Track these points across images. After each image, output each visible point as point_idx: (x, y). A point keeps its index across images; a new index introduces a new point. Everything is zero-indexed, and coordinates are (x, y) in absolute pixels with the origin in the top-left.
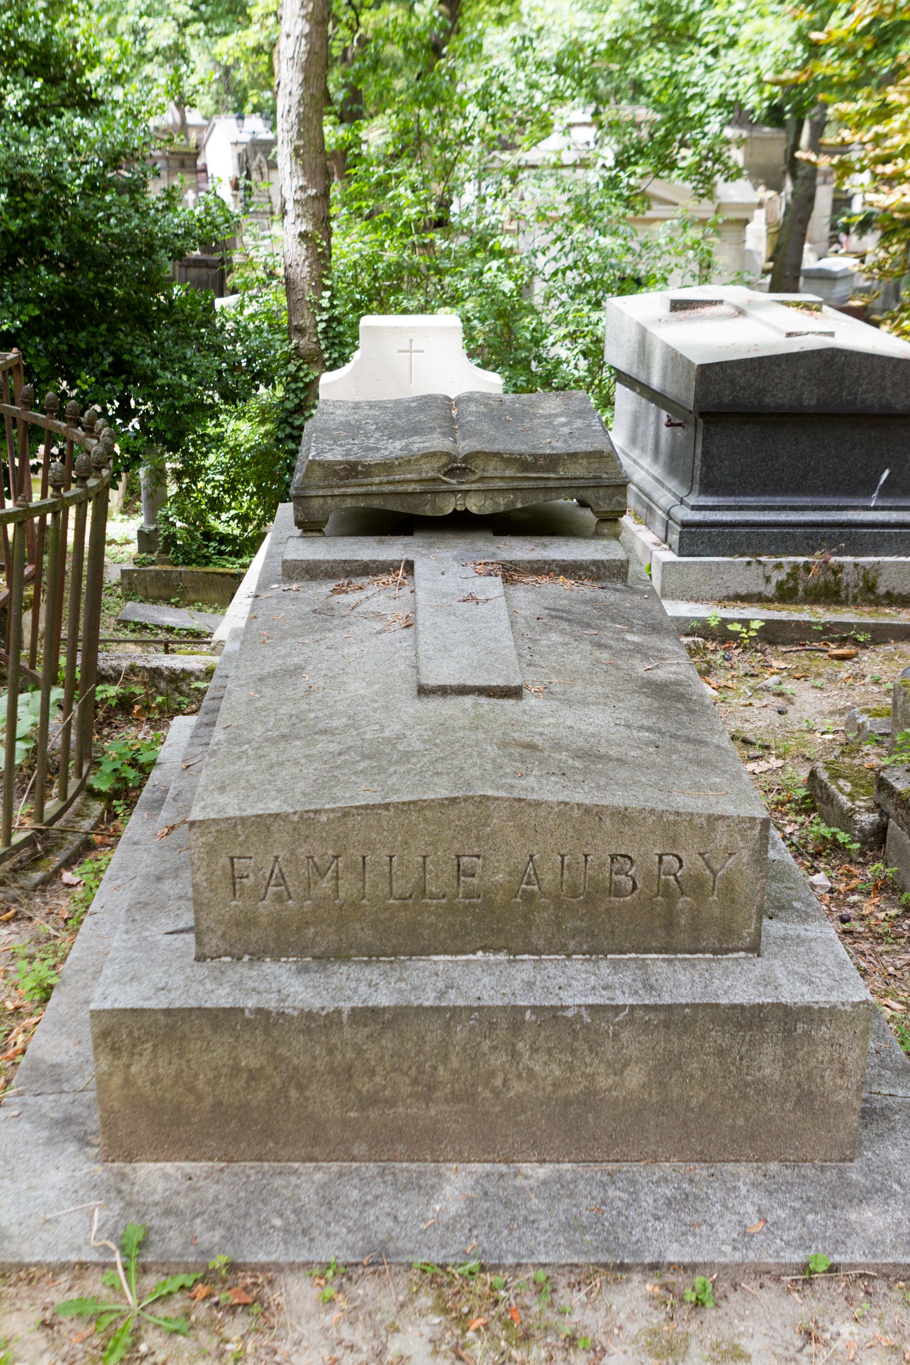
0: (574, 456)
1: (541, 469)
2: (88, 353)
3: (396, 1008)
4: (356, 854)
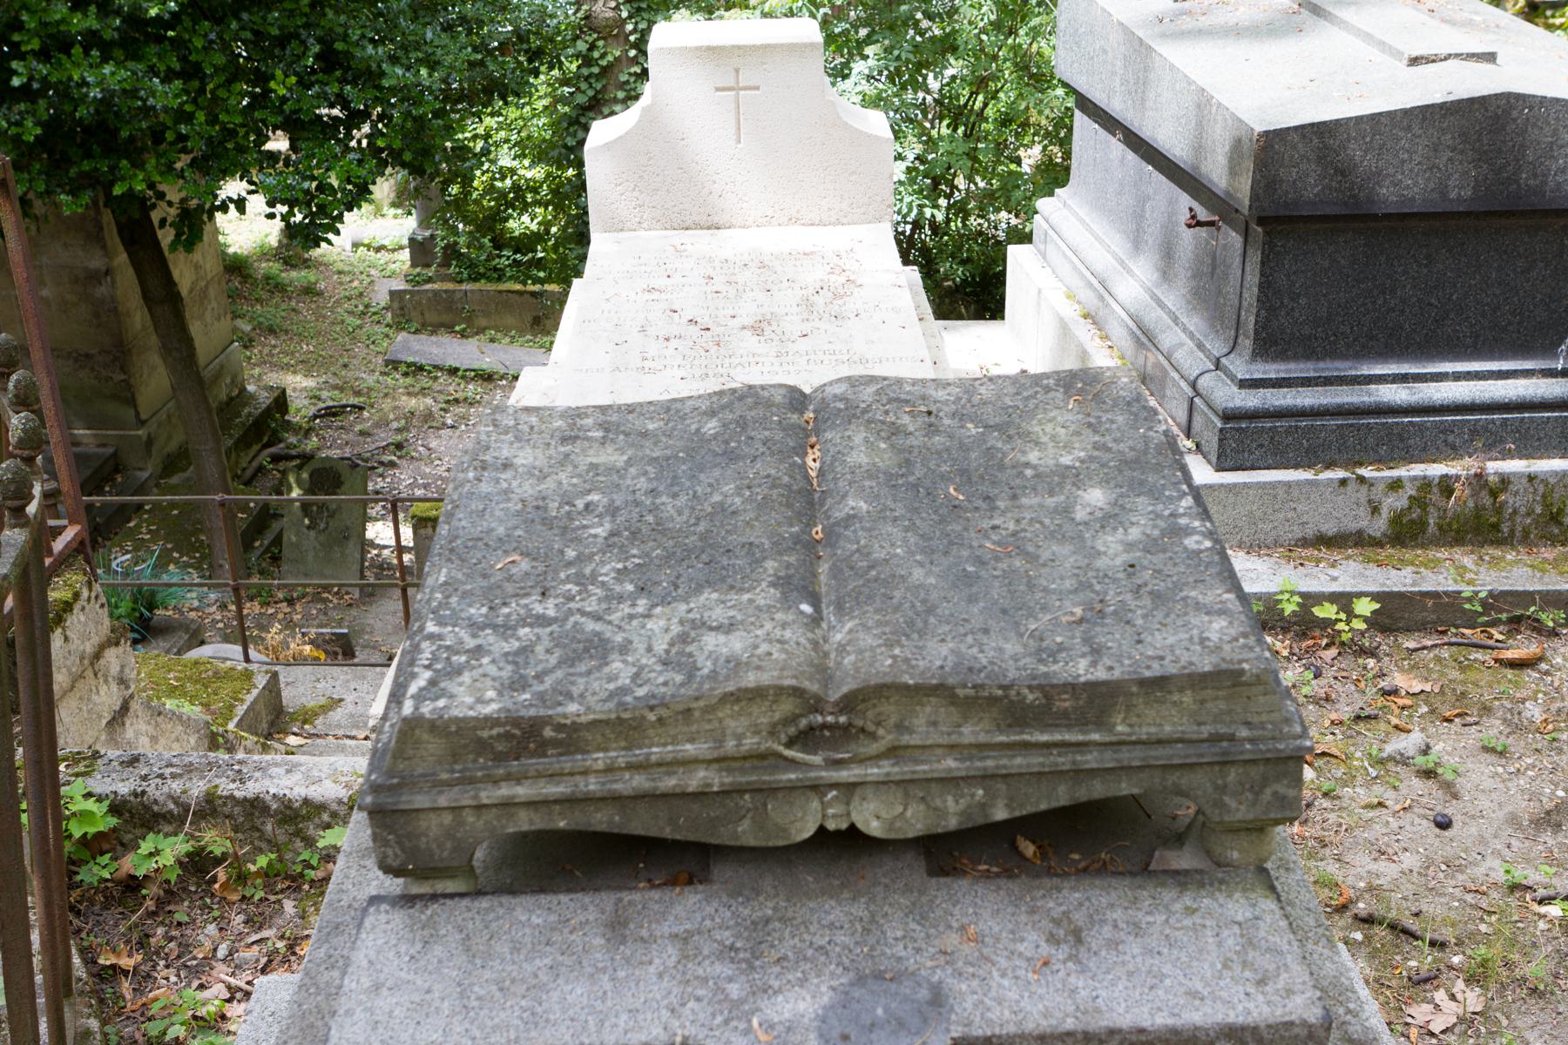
0: (1160, 684)
1: (1066, 720)
2: (282, 41)
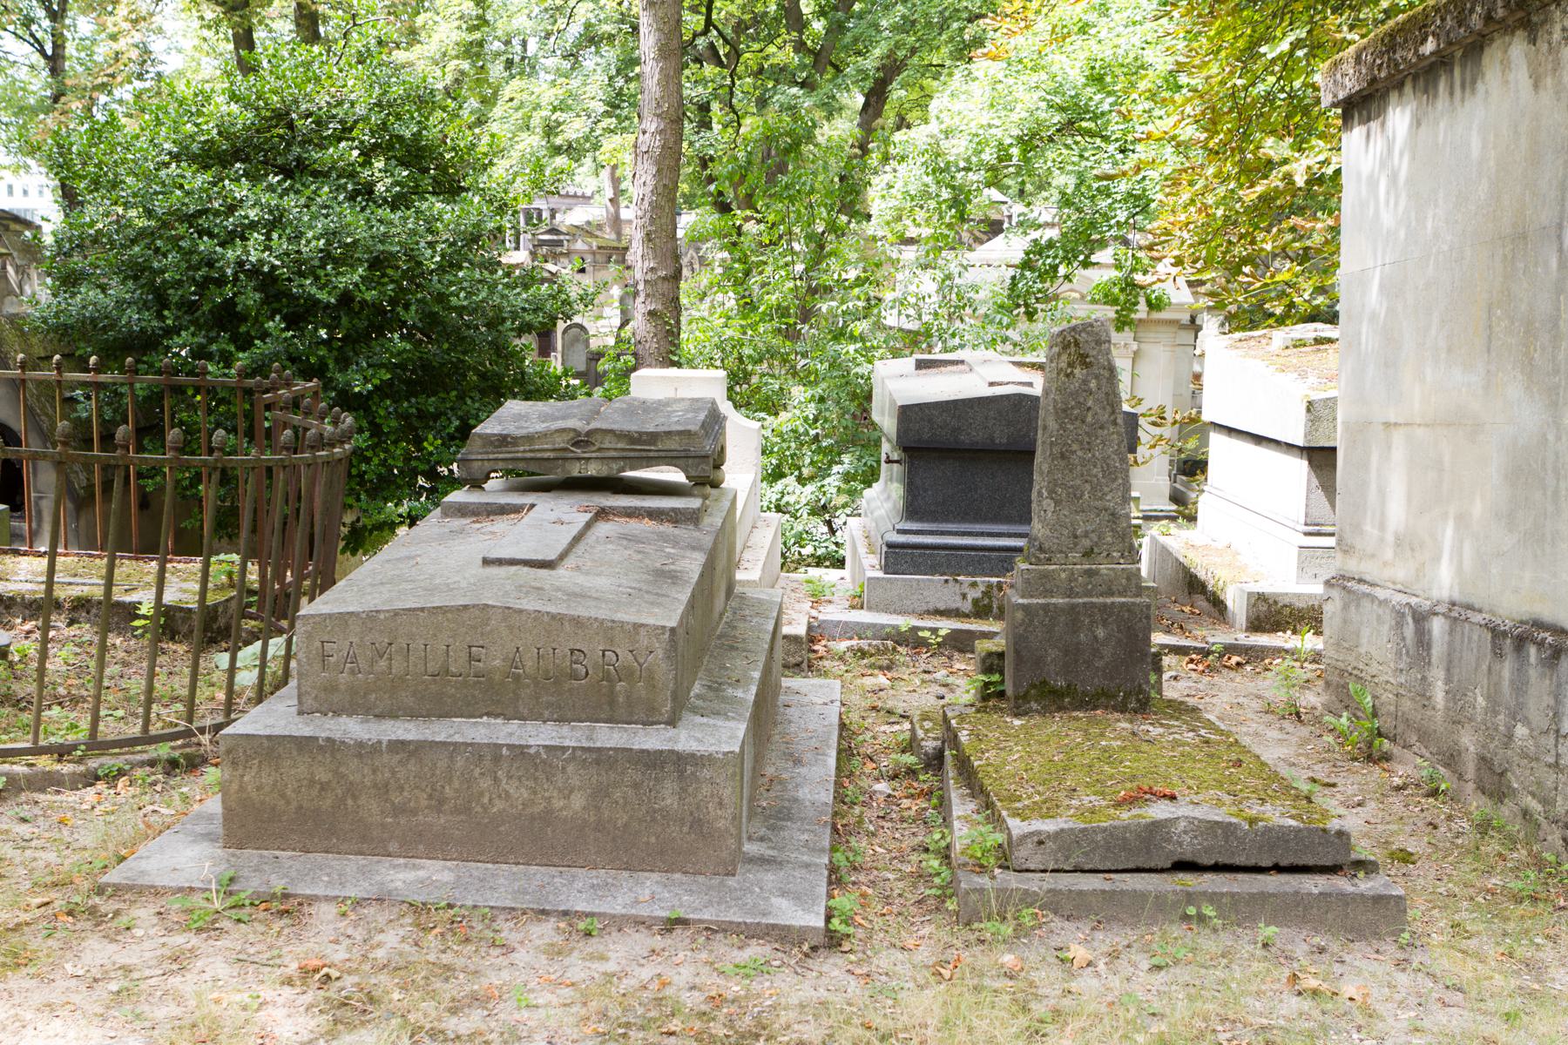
0: (669, 433)
1: (645, 443)
2: (436, 417)
3: (418, 741)
4: (403, 642)
